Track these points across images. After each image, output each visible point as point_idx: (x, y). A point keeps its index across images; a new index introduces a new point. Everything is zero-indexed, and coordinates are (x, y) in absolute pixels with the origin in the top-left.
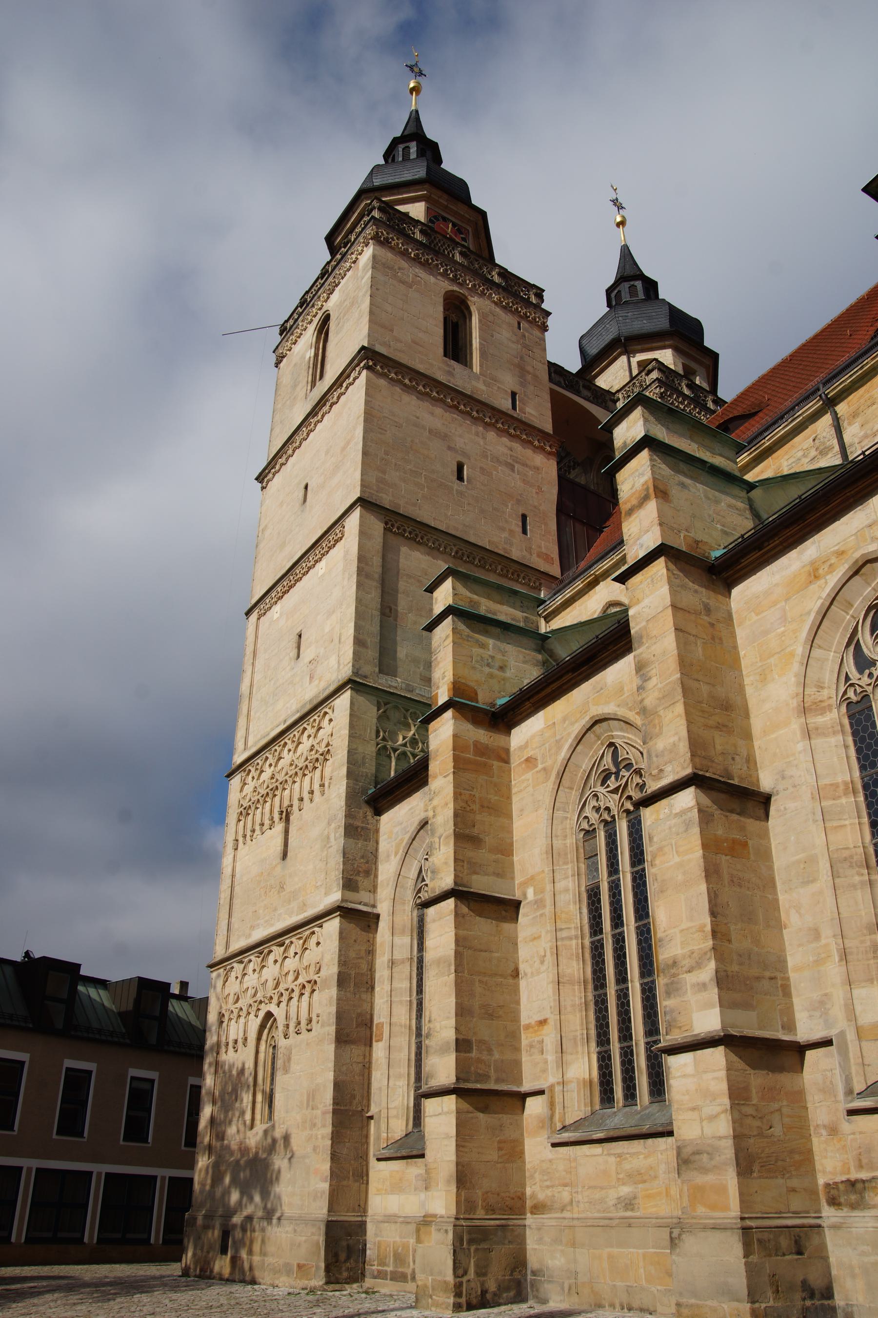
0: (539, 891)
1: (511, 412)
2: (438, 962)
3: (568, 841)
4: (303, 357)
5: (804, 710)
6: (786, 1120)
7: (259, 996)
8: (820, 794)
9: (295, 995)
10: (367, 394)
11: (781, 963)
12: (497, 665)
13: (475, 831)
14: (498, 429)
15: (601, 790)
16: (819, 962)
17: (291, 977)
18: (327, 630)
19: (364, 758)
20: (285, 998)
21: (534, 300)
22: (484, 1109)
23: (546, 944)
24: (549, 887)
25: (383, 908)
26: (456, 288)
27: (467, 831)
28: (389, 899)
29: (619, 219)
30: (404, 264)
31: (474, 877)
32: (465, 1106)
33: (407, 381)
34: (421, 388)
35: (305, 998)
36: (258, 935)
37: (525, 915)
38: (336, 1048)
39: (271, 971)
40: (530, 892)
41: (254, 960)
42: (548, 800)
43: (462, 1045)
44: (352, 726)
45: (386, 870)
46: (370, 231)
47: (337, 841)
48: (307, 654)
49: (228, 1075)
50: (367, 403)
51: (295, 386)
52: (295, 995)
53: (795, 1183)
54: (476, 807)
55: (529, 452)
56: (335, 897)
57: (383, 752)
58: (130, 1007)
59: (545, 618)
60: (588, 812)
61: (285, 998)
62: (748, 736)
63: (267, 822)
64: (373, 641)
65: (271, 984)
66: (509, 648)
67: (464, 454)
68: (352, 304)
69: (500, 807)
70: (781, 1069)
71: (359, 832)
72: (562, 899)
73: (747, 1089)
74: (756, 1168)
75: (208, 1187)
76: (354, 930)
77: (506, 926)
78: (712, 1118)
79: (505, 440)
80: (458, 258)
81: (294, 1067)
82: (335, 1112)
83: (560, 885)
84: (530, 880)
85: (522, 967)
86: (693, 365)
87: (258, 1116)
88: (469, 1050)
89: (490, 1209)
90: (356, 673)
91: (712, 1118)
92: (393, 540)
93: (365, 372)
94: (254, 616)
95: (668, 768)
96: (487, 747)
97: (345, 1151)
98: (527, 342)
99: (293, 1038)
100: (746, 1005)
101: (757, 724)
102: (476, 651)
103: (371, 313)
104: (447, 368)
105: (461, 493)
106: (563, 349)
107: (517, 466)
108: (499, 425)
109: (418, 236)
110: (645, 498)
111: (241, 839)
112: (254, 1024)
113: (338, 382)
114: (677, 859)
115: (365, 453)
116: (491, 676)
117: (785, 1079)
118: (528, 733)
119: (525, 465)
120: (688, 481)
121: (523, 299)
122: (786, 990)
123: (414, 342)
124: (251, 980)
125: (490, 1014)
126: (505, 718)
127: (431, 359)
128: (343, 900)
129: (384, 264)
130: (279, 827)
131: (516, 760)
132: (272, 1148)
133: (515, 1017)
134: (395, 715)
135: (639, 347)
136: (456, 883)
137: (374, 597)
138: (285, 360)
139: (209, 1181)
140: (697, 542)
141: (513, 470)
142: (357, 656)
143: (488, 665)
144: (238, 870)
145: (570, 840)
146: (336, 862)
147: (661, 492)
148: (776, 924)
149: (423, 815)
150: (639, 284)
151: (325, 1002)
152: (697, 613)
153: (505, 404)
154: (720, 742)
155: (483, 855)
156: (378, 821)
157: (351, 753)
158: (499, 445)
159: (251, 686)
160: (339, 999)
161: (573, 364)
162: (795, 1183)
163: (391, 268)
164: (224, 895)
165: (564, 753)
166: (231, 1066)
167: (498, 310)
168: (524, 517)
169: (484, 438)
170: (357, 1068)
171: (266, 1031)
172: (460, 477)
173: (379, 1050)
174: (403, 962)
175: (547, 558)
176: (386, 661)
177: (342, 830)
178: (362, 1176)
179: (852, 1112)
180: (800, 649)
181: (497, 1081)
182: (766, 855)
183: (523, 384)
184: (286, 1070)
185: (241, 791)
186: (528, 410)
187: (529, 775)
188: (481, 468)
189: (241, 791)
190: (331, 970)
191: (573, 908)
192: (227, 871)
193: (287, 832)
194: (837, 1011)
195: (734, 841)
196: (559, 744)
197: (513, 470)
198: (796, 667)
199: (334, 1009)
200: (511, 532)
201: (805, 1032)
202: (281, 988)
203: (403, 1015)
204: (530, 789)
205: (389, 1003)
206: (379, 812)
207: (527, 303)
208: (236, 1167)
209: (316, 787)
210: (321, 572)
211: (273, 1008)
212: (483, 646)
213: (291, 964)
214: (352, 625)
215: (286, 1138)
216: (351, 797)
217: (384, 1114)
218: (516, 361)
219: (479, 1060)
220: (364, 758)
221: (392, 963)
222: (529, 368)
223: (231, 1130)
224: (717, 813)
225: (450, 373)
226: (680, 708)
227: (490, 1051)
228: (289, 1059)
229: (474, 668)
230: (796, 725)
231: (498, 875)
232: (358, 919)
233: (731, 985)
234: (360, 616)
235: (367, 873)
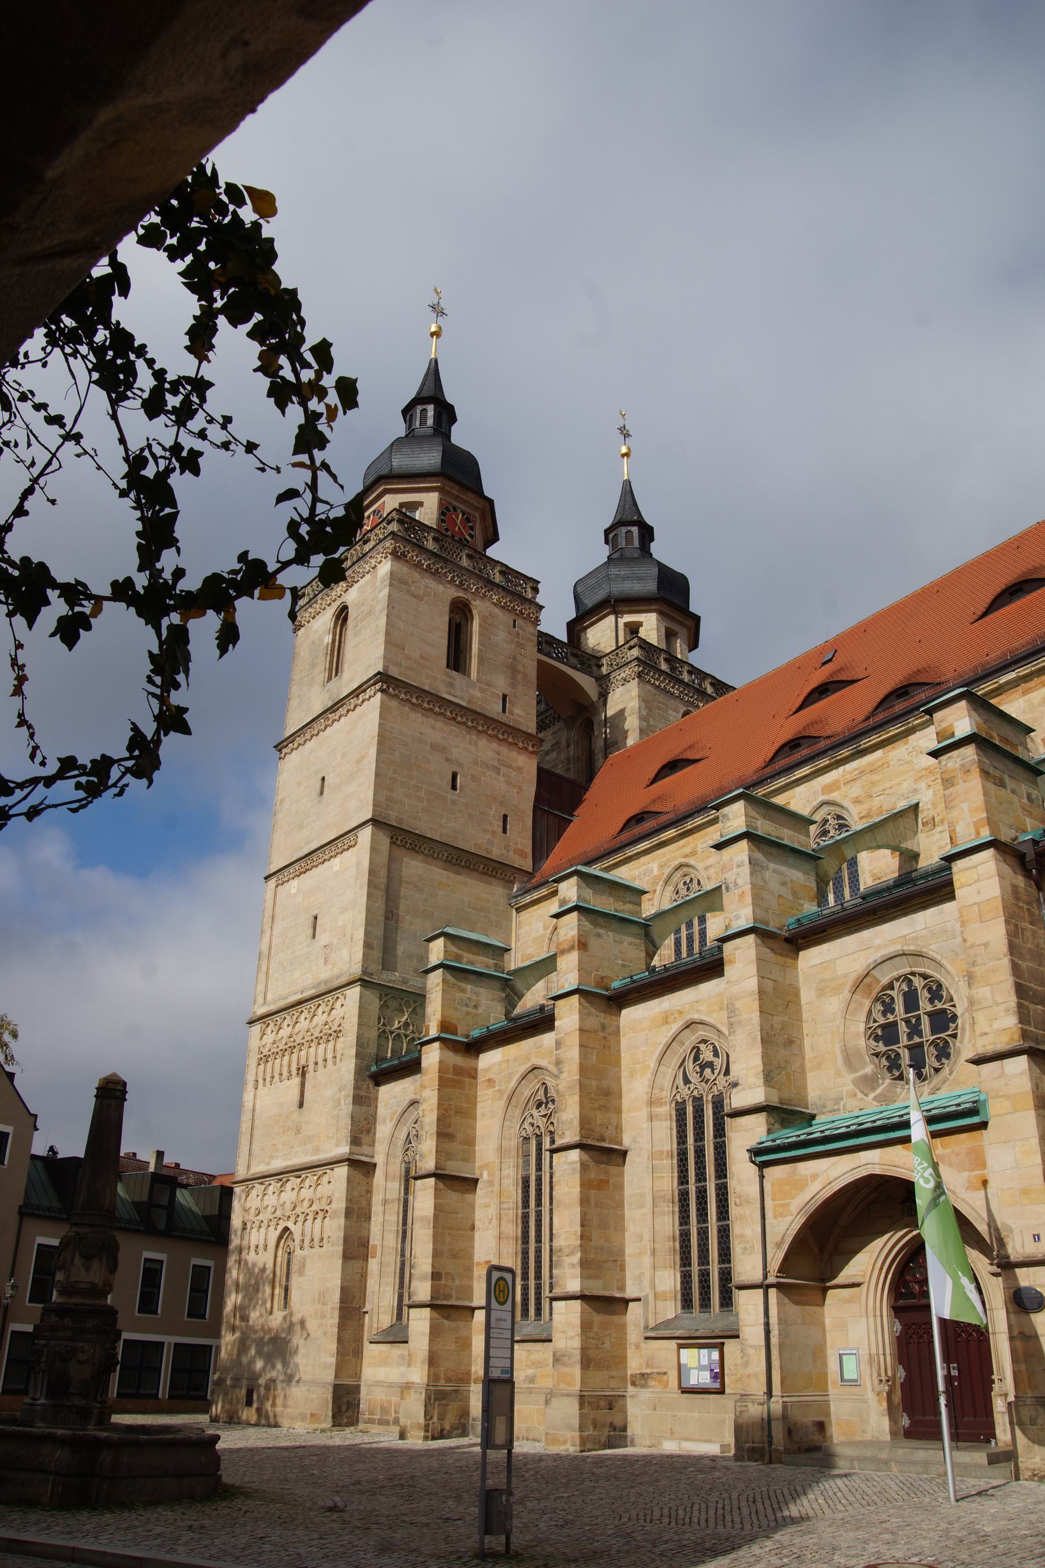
0: (490, 1174)
1: (502, 718)
2: (422, 1219)
3: (512, 1143)
4: (321, 638)
5: (651, 1103)
6: (613, 1340)
7: (278, 1214)
8: (653, 1156)
9: (310, 1217)
10: (381, 717)
11: (621, 1252)
12: (473, 1004)
13: (451, 1130)
14: (489, 735)
15: (535, 1112)
16: (640, 1254)
17: (306, 1204)
18: (340, 924)
19: (368, 1041)
20: (301, 1218)
22: (447, 1318)
23: (493, 1211)
24: (497, 1173)
25: (379, 1159)
26: (461, 594)
27: (445, 1131)
28: (383, 1153)
29: (624, 450)
30: (416, 575)
31: (449, 1162)
32: (436, 1315)
33: (414, 700)
34: (425, 705)
35: (318, 1221)
36: (278, 1164)
37: (481, 1189)
38: (343, 1262)
39: (288, 1196)
40: (485, 1174)
41: (274, 1185)
42: (500, 1113)
43: (436, 1276)
44: (360, 1016)
45: (383, 1130)
46: (389, 544)
47: (347, 1107)
48: (323, 938)
49: (250, 1272)
50: (381, 725)
51: (313, 666)
52: (310, 1217)
53: (614, 1373)
54: (452, 1113)
55: (514, 754)
57: (383, 1035)
58: (145, 1198)
59: (516, 909)
60: (526, 1125)
61: (301, 1218)
62: (619, 1111)
63: (285, 1073)
64: (377, 943)
65: (288, 1206)
66: (482, 990)
67: (460, 764)
68: (370, 613)
69: (468, 1113)
70: (613, 1313)
71: (363, 1100)
72: (505, 1182)
73: (591, 1323)
74: (592, 1365)
75: (235, 1357)
76: (359, 1176)
77: (468, 1196)
78: (572, 1338)
79: (494, 745)
80: (465, 562)
81: (308, 1272)
82: (341, 1308)
83: (505, 1173)
84: (486, 1166)
85: (477, 1224)
86: (676, 627)
87: (276, 1305)
88: (440, 1279)
89: (449, 1380)
90: (364, 972)
91: (572, 1338)
92: (399, 852)
93: (379, 694)
94: (272, 882)
95: (567, 1133)
96: (462, 1068)
97: (347, 1336)
98: (521, 641)
99: (307, 1251)
100: (597, 1277)
101: (625, 1104)
102: (459, 995)
103: (387, 633)
104: (448, 680)
105: (454, 802)
106: (555, 618)
107: (502, 768)
108: (490, 732)
109: (430, 545)
110: (572, 948)
111: (261, 1081)
112: (273, 1235)
113: (356, 693)
114: (567, 1190)
115: (377, 775)
116: (468, 1013)
117: (615, 1318)
118: (490, 1060)
119: (509, 767)
120: (602, 931)
121: (519, 591)
122: (622, 1268)
123: (422, 657)
124: (271, 1200)
125: (455, 1256)
126: (475, 1047)
127: (434, 676)
128: (351, 1153)
129: (399, 580)
130: (296, 1080)
131: (481, 1078)
133: (471, 1257)
134: (393, 1004)
135: (626, 609)
136: (436, 1168)
137: (380, 904)
138: (303, 629)
139: (235, 1352)
140: (602, 978)
141: (499, 774)
142: (365, 957)
143: (466, 1005)
144: (258, 1106)
145: (513, 1143)
146: (345, 1124)
147: (582, 945)
148: (620, 1227)
149: (413, 1097)
150: (635, 530)
151: (335, 1227)
152: (596, 1031)
153: (494, 709)
154: (600, 1117)
155: (455, 1147)
156: (377, 1091)
157: (359, 1038)
158: (487, 749)
159: (270, 947)
160: (345, 1227)
161: (562, 636)
162: (614, 1373)
163: (406, 583)
164: (245, 1127)
165: (513, 1083)
166: (254, 1265)
167: (497, 610)
168: (505, 817)
169: (476, 745)
170: (357, 1277)
171: (283, 1241)
173: (373, 1264)
174: (393, 1201)
175: (522, 854)
176: (388, 962)
177: (351, 1099)
178: (358, 1353)
179: (647, 1338)
180: (652, 1064)
181: (457, 1299)
182: (620, 1187)
183: (513, 685)
184: (301, 1273)
185: (261, 1039)
186: (517, 711)
187: (490, 1091)
188: (473, 776)
189: (261, 1039)
190: (340, 1204)
191: (512, 1189)
192: (248, 1105)
193: (303, 1085)
194: (646, 1283)
195: (601, 1180)
196: (510, 1076)
197: (499, 774)
198: (649, 1075)
199: (342, 1234)
200: (494, 833)
201: (629, 1294)
202: (298, 1210)
203: (392, 1240)
204: (490, 1101)
205: (382, 1230)
206: (378, 1084)
207: (524, 600)
208: (260, 1343)
209: (330, 1056)
210: (336, 869)
211: (290, 1224)
212: (463, 991)
213: (306, 1193)
214: (362, 930)
215: (302, 1322)
216: (359, 1073)
217: (375, 1311)
218: (509, 661)
219: (446, 1286)
220: (368, 1041)
221: (385, 1201)
222: (520, 668)
223: (254, 1315)
224: (592, 1164)
225: (451, 685)
226: (577, 1098)
227: (453, 1279)
228: (304, 1266)
229: (456, 1009)
230: (644, 1112)
231: (464, 1160)
232: (361, 1168)
233: (588, 1266)
234: (369, 922)
235: (368, 1131)
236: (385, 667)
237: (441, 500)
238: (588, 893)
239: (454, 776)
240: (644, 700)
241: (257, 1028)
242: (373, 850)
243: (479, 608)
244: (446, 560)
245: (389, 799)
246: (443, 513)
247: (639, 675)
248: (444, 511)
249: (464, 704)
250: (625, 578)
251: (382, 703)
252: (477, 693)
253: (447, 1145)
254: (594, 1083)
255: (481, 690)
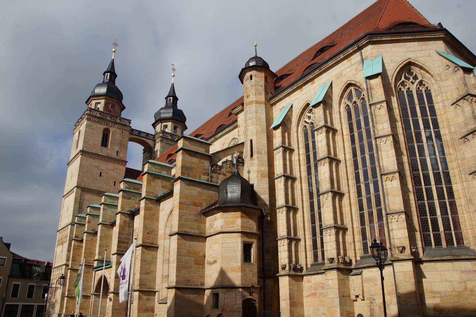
21: (128, 124)
29: (173, 75)
36: (58, 265)
46: (86, 116)
56: (65, 262)
67: (102, 170)
79: (113, 164)
80: (109, 118)
92: (83, 193)
105: (100, 180)
112: (56, 280)
132: (55, 302)
137: (78, 206)
155: (76, 263)
163: (90, 126)
167: (117, 130)
168: (115, 182)
172: (101, 176)
183: (120, 148)
186: (121, 155)
200: (111, 186)
207: (125, 125)
222: (123, 143)
225: (102, 150)
234: (74, 210)
236: (83, 149)
237: (105, 102)
238: (92, 210)
239: (101, 173)
240: (162, 147)
241: (58, 233)
242: (76, 193)
243: (112, 130)
244: (103, 119)
245: (81, 180)
246: (106, 105)
247: (161, 141)
248: (106, 104)
249: (105, 155)
250: (165, 113)
251: (81, 158)
252: (109, 152)
253: (74, 262)
254: (88, 252)
255: (111, 151)
